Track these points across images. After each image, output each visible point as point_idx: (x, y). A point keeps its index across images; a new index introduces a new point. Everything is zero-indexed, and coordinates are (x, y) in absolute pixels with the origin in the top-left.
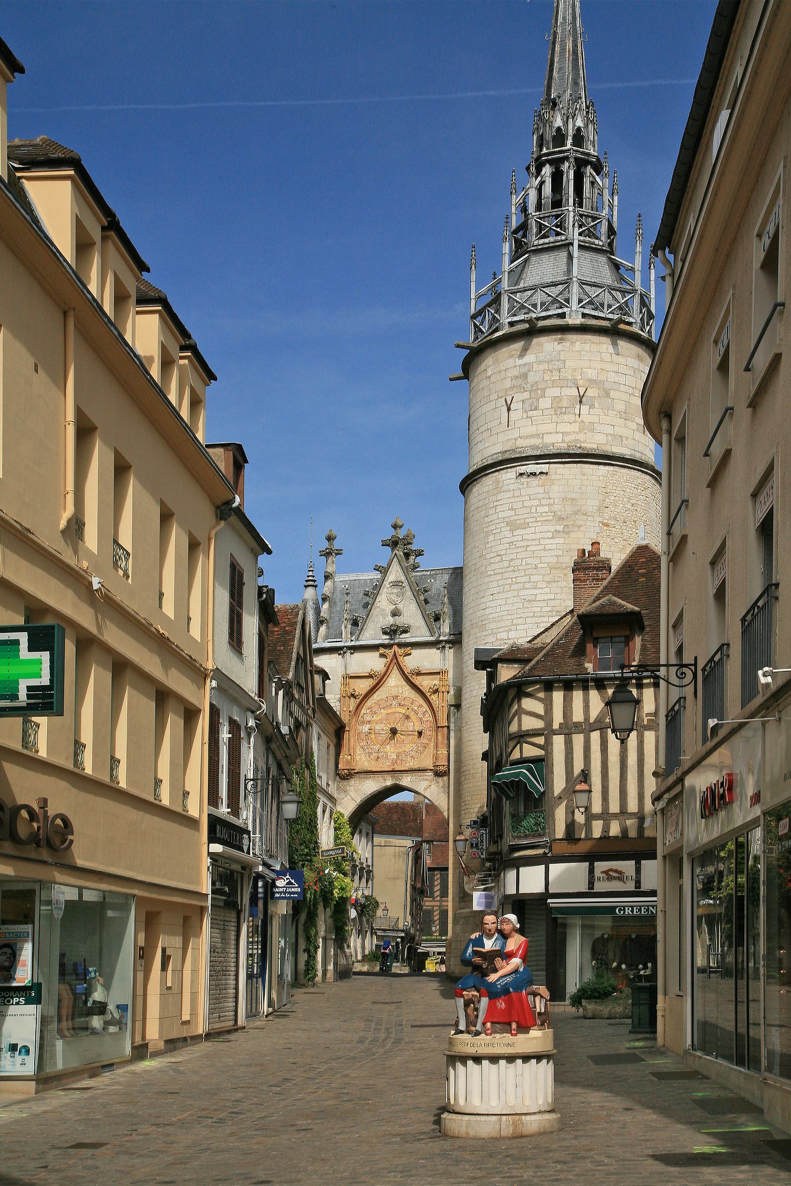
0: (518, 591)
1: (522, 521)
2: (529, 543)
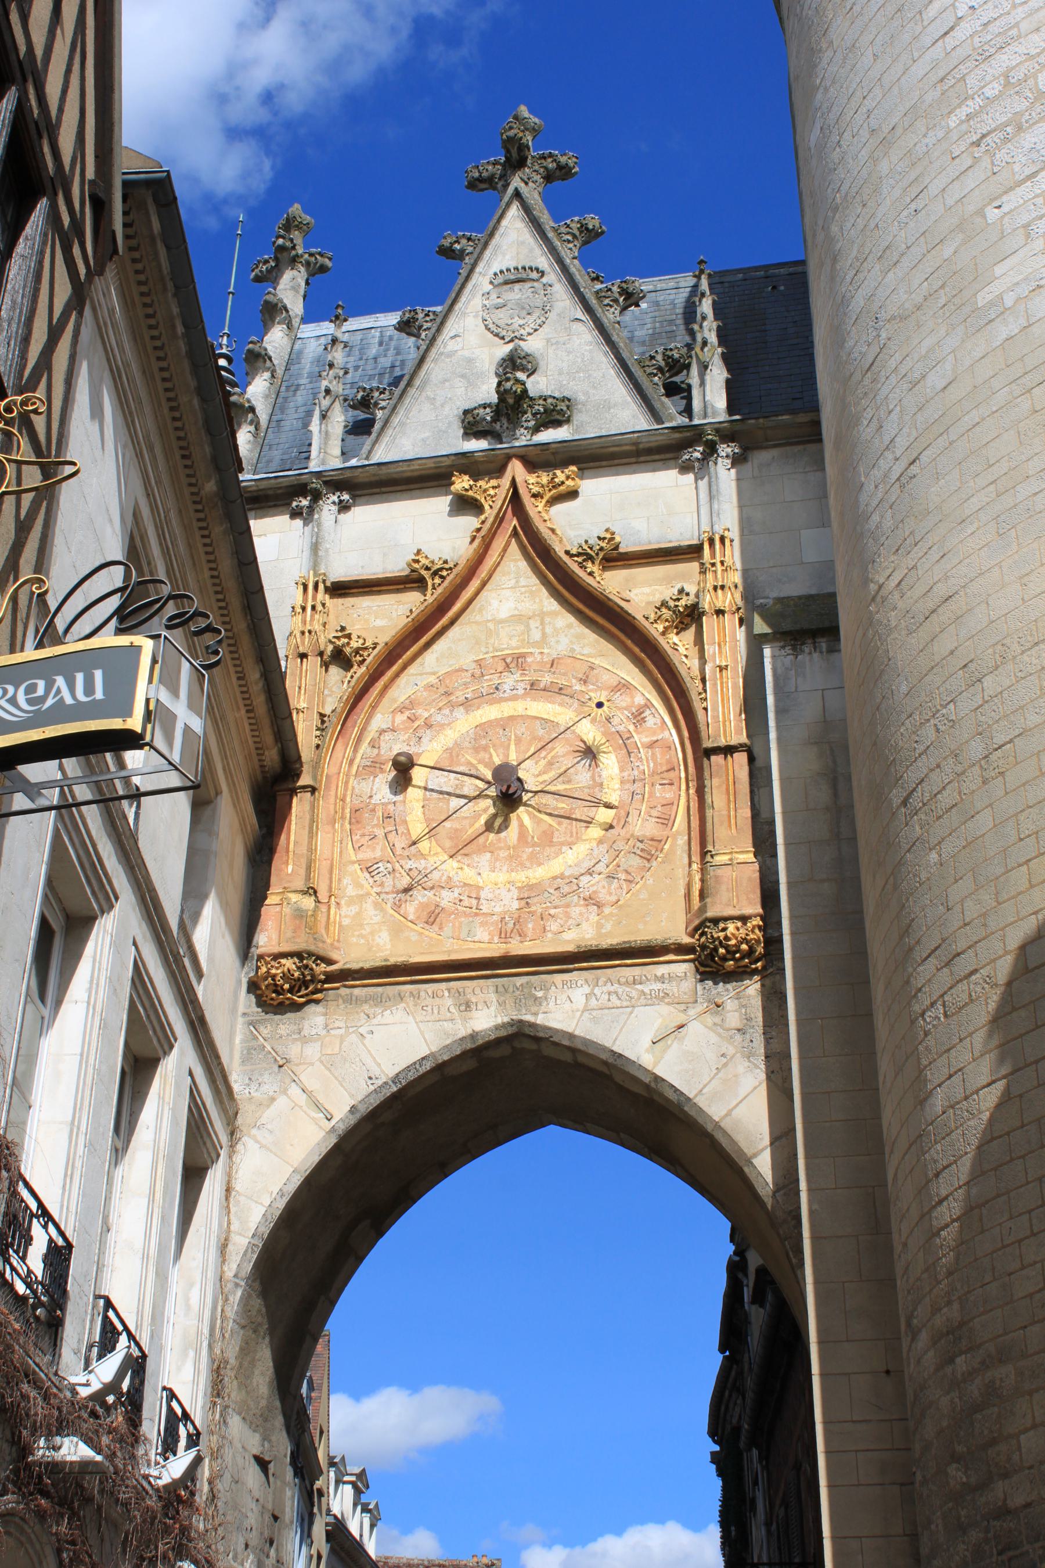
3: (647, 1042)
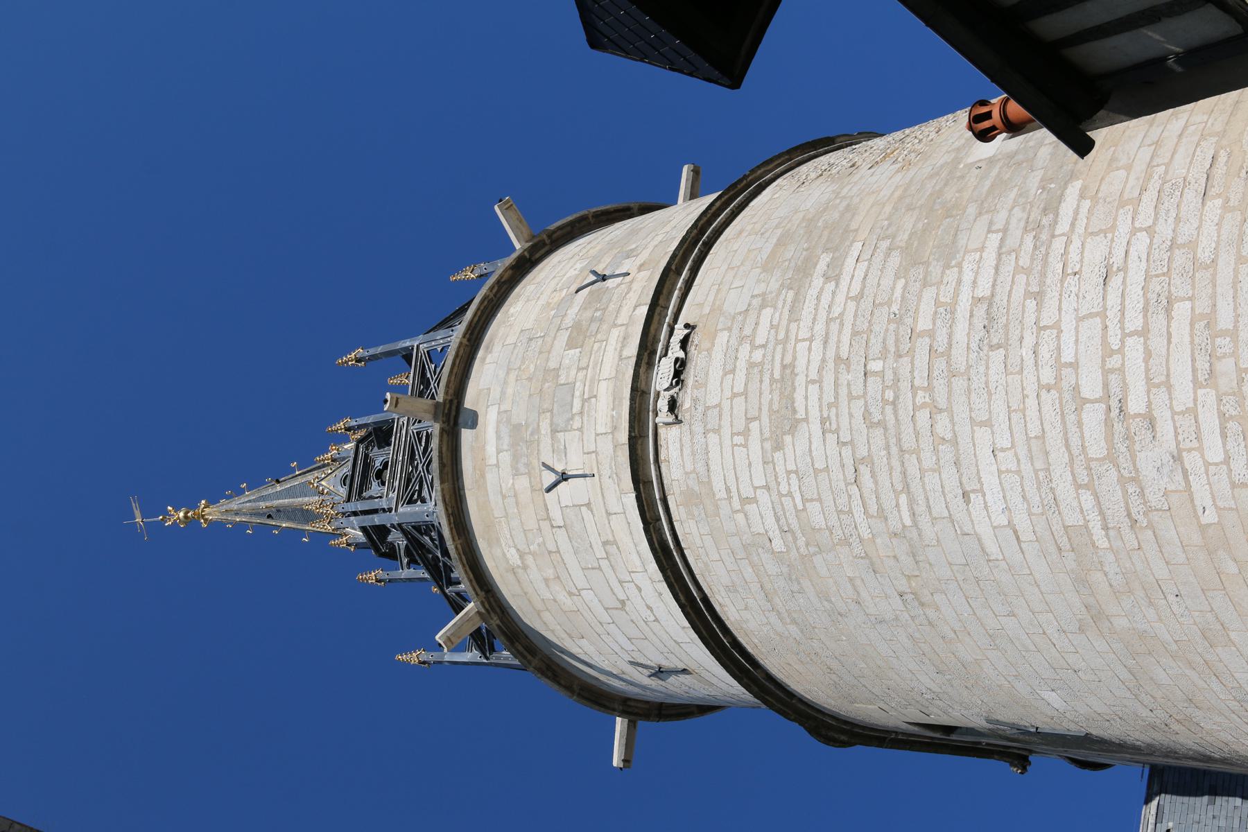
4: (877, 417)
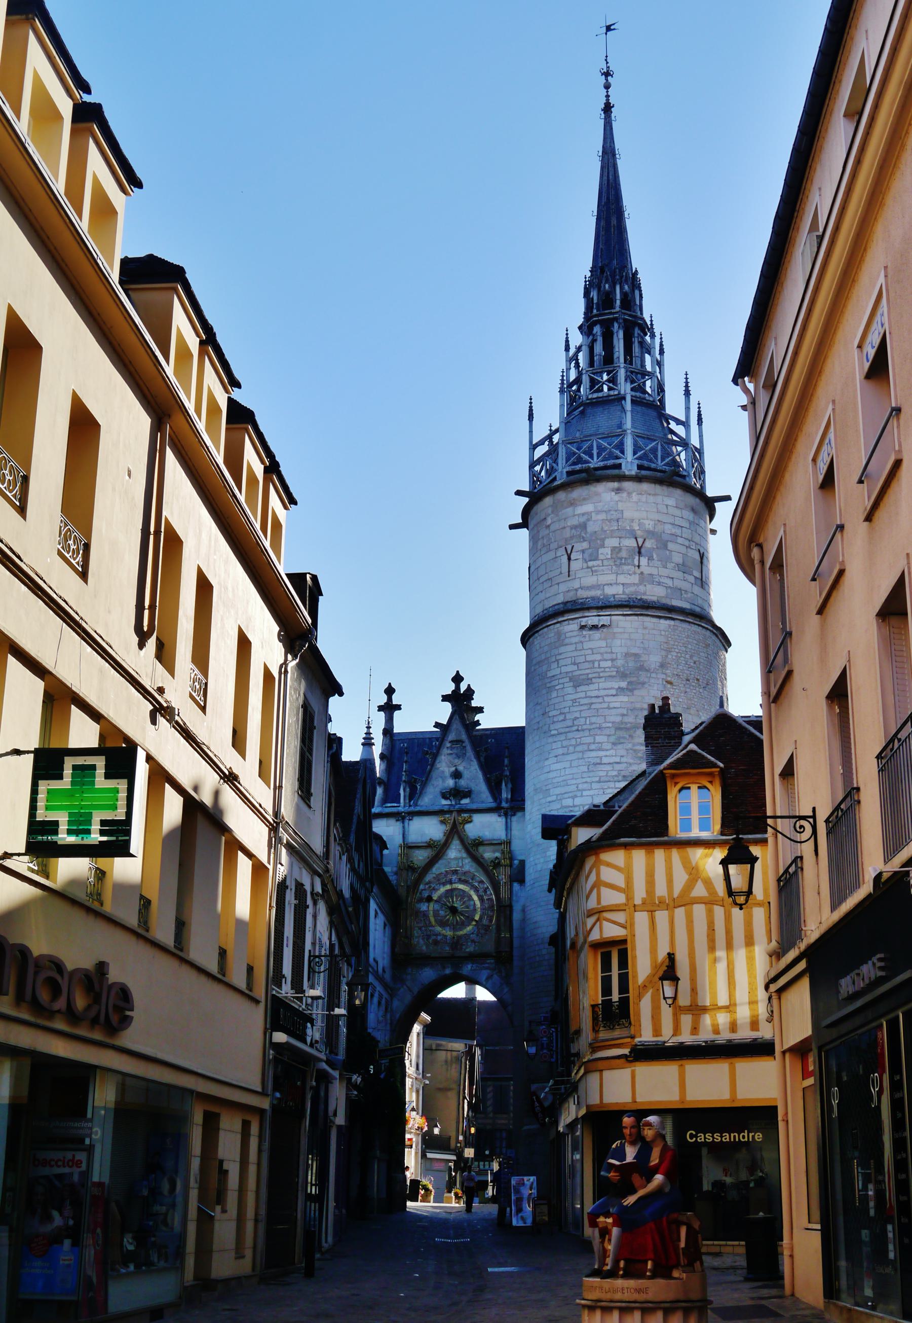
0: (582, 752)
1: (584, 677)
2: (594, 700)
3: (484, 978)
4: (575, 722)
